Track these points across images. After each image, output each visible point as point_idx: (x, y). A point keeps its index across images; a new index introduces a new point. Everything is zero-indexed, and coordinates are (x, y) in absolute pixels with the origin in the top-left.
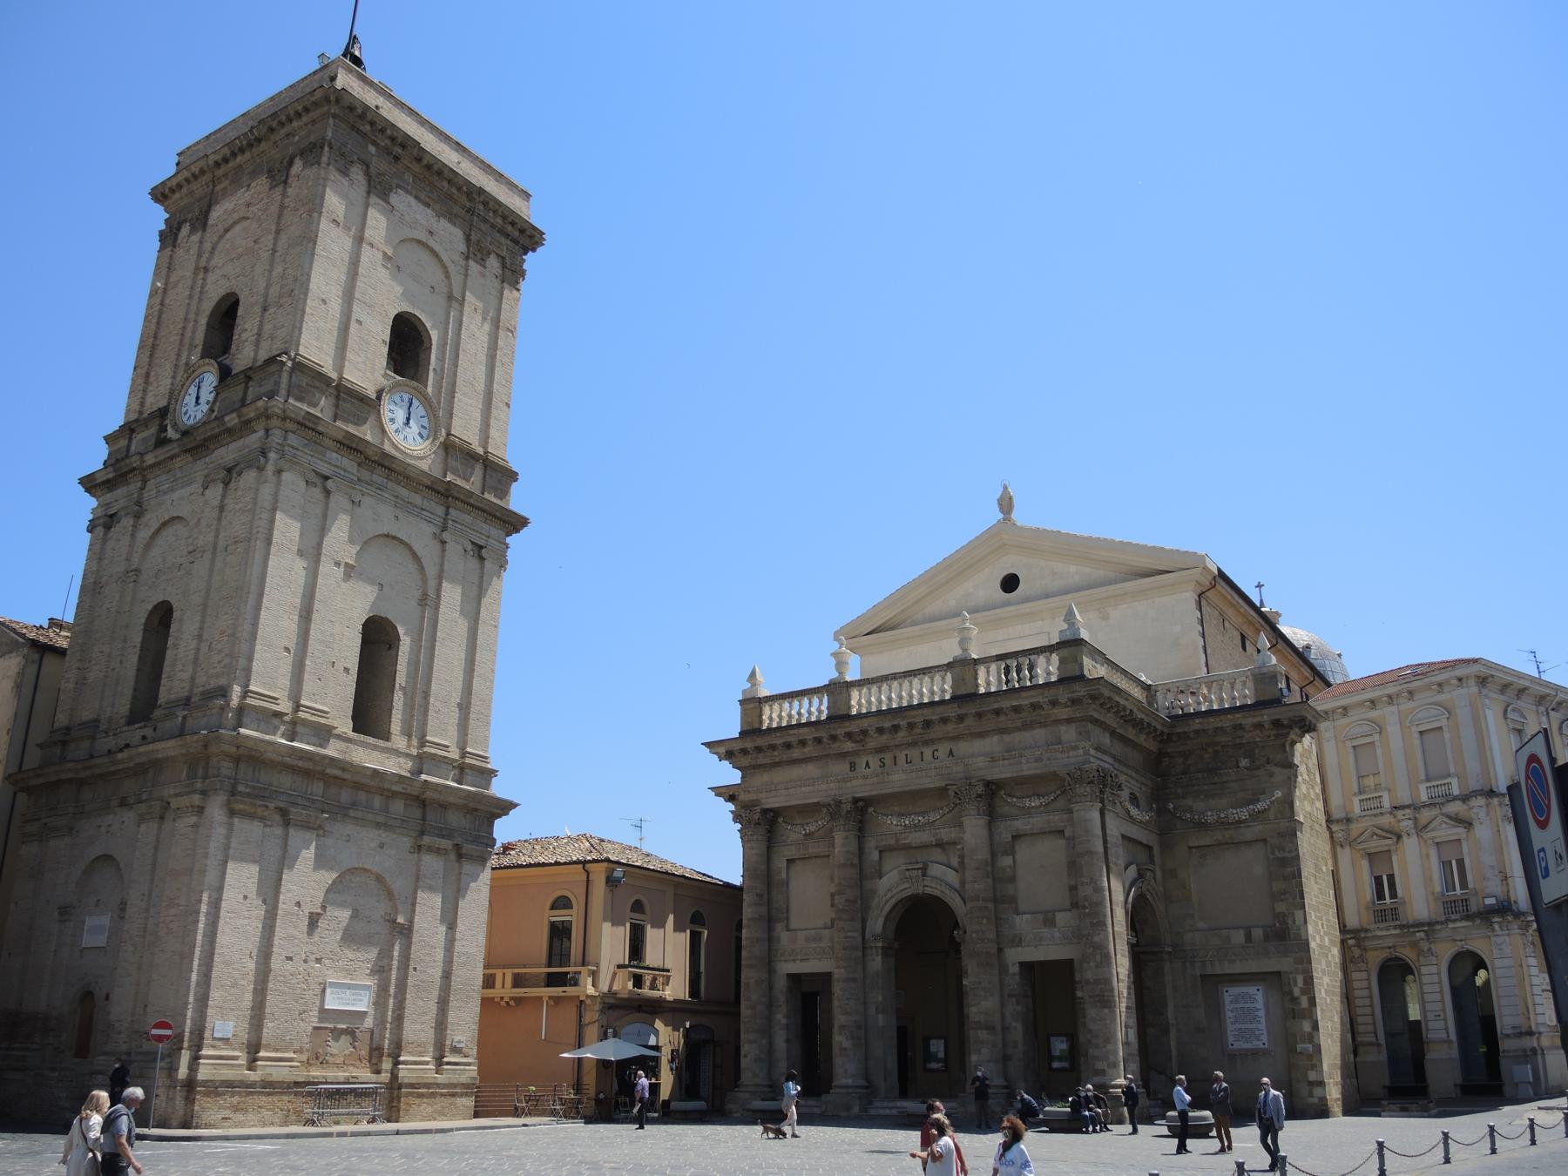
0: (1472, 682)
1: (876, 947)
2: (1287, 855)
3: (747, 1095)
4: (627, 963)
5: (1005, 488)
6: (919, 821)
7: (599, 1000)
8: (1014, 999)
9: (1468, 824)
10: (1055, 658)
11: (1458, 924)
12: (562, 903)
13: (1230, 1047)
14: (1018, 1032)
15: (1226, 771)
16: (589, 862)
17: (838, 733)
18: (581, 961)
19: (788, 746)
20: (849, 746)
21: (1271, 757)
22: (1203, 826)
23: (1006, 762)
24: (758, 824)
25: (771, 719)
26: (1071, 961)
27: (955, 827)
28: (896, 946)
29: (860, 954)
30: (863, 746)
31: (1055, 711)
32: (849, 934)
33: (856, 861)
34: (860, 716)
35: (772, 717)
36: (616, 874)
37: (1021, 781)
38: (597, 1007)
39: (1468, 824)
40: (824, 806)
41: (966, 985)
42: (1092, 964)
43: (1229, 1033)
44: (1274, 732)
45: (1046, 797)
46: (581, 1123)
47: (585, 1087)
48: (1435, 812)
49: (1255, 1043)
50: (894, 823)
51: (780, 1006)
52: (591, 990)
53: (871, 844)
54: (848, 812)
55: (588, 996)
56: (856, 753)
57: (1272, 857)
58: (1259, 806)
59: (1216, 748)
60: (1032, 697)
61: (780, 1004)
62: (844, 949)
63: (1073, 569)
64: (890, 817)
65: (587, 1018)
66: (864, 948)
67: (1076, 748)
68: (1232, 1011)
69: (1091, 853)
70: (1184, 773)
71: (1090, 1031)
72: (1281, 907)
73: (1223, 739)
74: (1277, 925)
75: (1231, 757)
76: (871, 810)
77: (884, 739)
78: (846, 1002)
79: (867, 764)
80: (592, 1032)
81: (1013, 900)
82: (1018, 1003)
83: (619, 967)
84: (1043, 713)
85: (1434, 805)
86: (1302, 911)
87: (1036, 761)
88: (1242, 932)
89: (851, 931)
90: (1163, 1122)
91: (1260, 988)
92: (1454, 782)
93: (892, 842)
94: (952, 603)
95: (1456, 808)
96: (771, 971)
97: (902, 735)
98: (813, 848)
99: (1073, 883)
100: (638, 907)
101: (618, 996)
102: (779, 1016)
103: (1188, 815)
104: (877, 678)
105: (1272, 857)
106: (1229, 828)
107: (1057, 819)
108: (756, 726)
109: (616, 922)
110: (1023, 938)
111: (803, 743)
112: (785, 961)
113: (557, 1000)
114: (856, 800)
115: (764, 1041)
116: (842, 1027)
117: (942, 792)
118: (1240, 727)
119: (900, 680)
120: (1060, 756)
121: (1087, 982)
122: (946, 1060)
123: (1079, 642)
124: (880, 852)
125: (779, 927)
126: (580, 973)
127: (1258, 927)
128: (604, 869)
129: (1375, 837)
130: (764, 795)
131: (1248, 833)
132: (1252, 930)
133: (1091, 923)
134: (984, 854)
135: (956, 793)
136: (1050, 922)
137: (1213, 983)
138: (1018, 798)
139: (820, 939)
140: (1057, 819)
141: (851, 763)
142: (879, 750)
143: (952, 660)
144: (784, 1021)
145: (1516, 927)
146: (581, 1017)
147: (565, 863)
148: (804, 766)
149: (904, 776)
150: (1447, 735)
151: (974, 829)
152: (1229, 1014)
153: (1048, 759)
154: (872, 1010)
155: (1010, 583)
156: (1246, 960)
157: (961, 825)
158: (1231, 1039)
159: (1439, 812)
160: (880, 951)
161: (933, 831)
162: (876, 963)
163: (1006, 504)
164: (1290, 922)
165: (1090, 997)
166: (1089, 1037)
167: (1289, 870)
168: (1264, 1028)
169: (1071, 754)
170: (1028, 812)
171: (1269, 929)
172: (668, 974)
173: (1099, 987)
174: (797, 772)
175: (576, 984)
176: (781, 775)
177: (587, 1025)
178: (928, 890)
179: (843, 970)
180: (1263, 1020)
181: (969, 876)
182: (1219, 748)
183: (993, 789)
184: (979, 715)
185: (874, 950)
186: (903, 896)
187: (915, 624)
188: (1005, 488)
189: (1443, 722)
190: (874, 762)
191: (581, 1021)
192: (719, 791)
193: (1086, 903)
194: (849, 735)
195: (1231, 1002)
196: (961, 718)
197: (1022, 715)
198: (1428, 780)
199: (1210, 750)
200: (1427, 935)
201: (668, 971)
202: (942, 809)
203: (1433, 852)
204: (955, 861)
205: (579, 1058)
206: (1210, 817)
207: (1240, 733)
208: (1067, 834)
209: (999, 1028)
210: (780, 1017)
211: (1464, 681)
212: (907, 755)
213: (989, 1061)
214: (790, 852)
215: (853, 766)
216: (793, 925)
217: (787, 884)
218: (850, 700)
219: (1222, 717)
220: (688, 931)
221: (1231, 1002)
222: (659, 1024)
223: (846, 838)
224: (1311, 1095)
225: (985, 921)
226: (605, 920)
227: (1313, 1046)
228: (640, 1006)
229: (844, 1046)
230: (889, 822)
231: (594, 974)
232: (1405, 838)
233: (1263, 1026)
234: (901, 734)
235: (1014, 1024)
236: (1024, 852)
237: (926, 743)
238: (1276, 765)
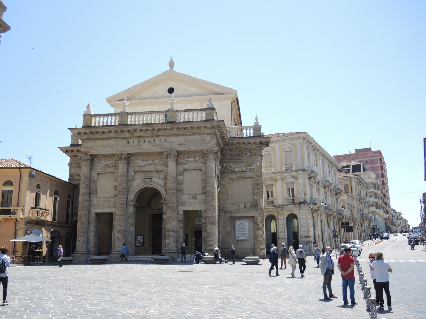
0: (302, 139)
1: (131, 205)
2: (259, 182)
3: (80, 255)
4: (34, 207)
5: (172, 59)
6: (150, 163)
7: (24, 220)
8: (180, 222)
9: (296, 178)
10: (204, 113)
11: (291, 206)
12: (9, 183)
13: (237, 238)
14: (181, 233)
15: (243, 156)
16: (22, 168)
17: (125, 129)
18: (17, 205)
19: (104, 133)
20: (127, 135)
21: (257, 153)
22: (234, 172)
23: (185, 145)
24: (88, 159)
25: (95, 123)
26: (200, 211)
27: (163, 165)
28: (137, 204)
29: (126, 206)
30: (133, 135)
31: (205, 130)
32: (123, 199)
33: (126, 175)
34: (131, 125)
35: (95, 122)
36: (33, 173)
37: (188, 152)
38: (24, 223)
39: (296, 178)
40: (116, 155)
41: (164, 218)
42: (211, 211)
43: (237, 234)
44: (259, 145)
45: (196, 158)
46: (22, 266)
47: (17, 252)
48: (287, 174)
49: (245, 237)
50: (141, 163)
51: (92, 224)
52: (22, 216)
53: (131, 170)
54: (125, 158)
55: (21, 219)
56: (129, 138)
57: (254, 182)
58: (252, 167)
59: (240, 149)
60: (198, 124)
61: (92, 223)
62: (121, 204)
63: (193, 89)
64: (139, 161)
65: (19, 226)
66: (127, 204)
67: (210, 143)
68: (238, 228)
69: (212, 176)
70: (230, 155)
71: (208, 232)
72: (256, 197)
73: (243, 146)
74: (254, 203)
75: (245, 152)
76: (132, 158)
77: (141, 134)
78: (120, 222)
79: (134, 142)
80: (21, 232)
81: (182, 190)
82: (182, 224)
83: (32, 208)
84: (200, 130)
85: (287, 172)
86: (262, 199)
87: (196, 146)
88: (244, 204)
89: (123, 199)
90: (244, 260)
91: (247, 221)
92: (294, 166)
93: (139, 169)
94: (150, 94)
95: (293, 173)
96: (90, 212)
97: (148, 133)
98: (108, 170)
99: (203, 186)
100: (38, 186)
101: (31, 219)
102: (92, 227)
103: (230, 168)
104: (139, 112)
105: (254, 182)
106: (242, 173)
108: (89, 125)
109: (31, 192)
110: (185, 203)
111: (110, 132)
112: (95, 208)
113: (6, 220)
114: (128, 154)
115: (86, 236)
116: (119, 231)
117: (161, 153)
118: (250, 143)
119: (148, 114)
120: (204, 145)
121: (208, 217)
122: (143, 243)
123: (213, 109)
124: (135, 172)
125: (93, 197)
126: (17, 210)
127: (248, 203)
128: (29, 171)
129: (269, 180)
130: (91, 149)
132: (247, 204)
133: (211, 198)
134: (174, 175)
135: (167, 154)
136: (195, 198)
137: (233, 219)
138: (187, 158)
139: (109, 201)
141: (127, 141)
142: (139, 137)
143: (168, 109)
144: (93, 229)
145: (307, 207)
146: (16, 226)
147: (11, 168)
148: (108, 140)
149: (147, 147)
150: (293, 153)
151: (172, 166)
152: (237, 229)
153: (200, 145)
154: (129, 226)
155: (171, 90)
156: (244, 212)
157: (167, 166)
158: (237, 236)
159: (288, 174)
160: (132, 206)
161: (155, 167)
162: (131, 209)
163: (172, 64)
164: (258, 202)
165: (210, 222)
166: (208, 234)
167: (259, 187)
168: (248, 233)
169: (208, 144)
170: (189, 162)
171: (252, 204)
172: (49, 211)
173: (213, 219)
174: (105, 142)
175: (15, 214)
176: (99, 143)
177: (19, 229)
178: (152, 186)
179: (120, 212)
180: (247, 231)
181: (169, 182)
182: (241, 149)
183: (179, 153)
184: (178, 129)
185: (130, 205)
186: (142, 188)
187: (136, 99)
188: (172, 59)
189: (292, 149)
190: (136, 141)
191: (16, 228)
192: (61, 149)
193: (210, 192)
194: (128, 131)
195: (238, 225)
196: (171, 129)
197: (193, 130)
198: (286, 165)
199: (239, 149)
200: (281, 209)
201: (48, 210)
202: (159, 159)
203: (285, 186)
204: (162, 177)
205: (15, 241)
206: (237, 170)
207: (249, 145)
208: (202, 170)
209: (176, 232)
210: (92, 228)
211: (300, 138)
213: (173, 242)
214: (99, 171)
215: (128, 142)
216: (98, 196)
217: (97, 182)
218: (128, 119)
219: (245, 139)
220: (53, 197)
221: (238, 225)
222: (43, 230)
223: (124, 167)
224: (261, 253)
225: (174, 197)
226: (28, 190)
227: (262, 239)
228: (37, 223)
229: (119, 237)
230: (139, 162)
231: (23, 210)
232: (278, 181)
233: (247, 232)
234: (148, 132)
235: (180, 230)
236: (187, 175)
237: (157, 136)
238: (258, 155)
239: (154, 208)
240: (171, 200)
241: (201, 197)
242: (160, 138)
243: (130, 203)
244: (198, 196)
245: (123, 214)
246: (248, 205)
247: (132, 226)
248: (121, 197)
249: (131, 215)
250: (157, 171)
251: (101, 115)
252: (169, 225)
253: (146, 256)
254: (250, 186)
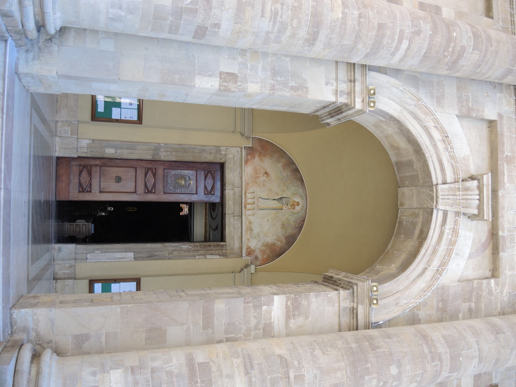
1: (351, 93)
32: (405, 45)
41: (270, 303)
62: (381, 27)
89: (408, 48)
239: (248, 170)
240: (400, 373)
243: (358, 87)
245: (322, 37)
247: (224, 90)
248: (418, 33)
249: (293, 88)
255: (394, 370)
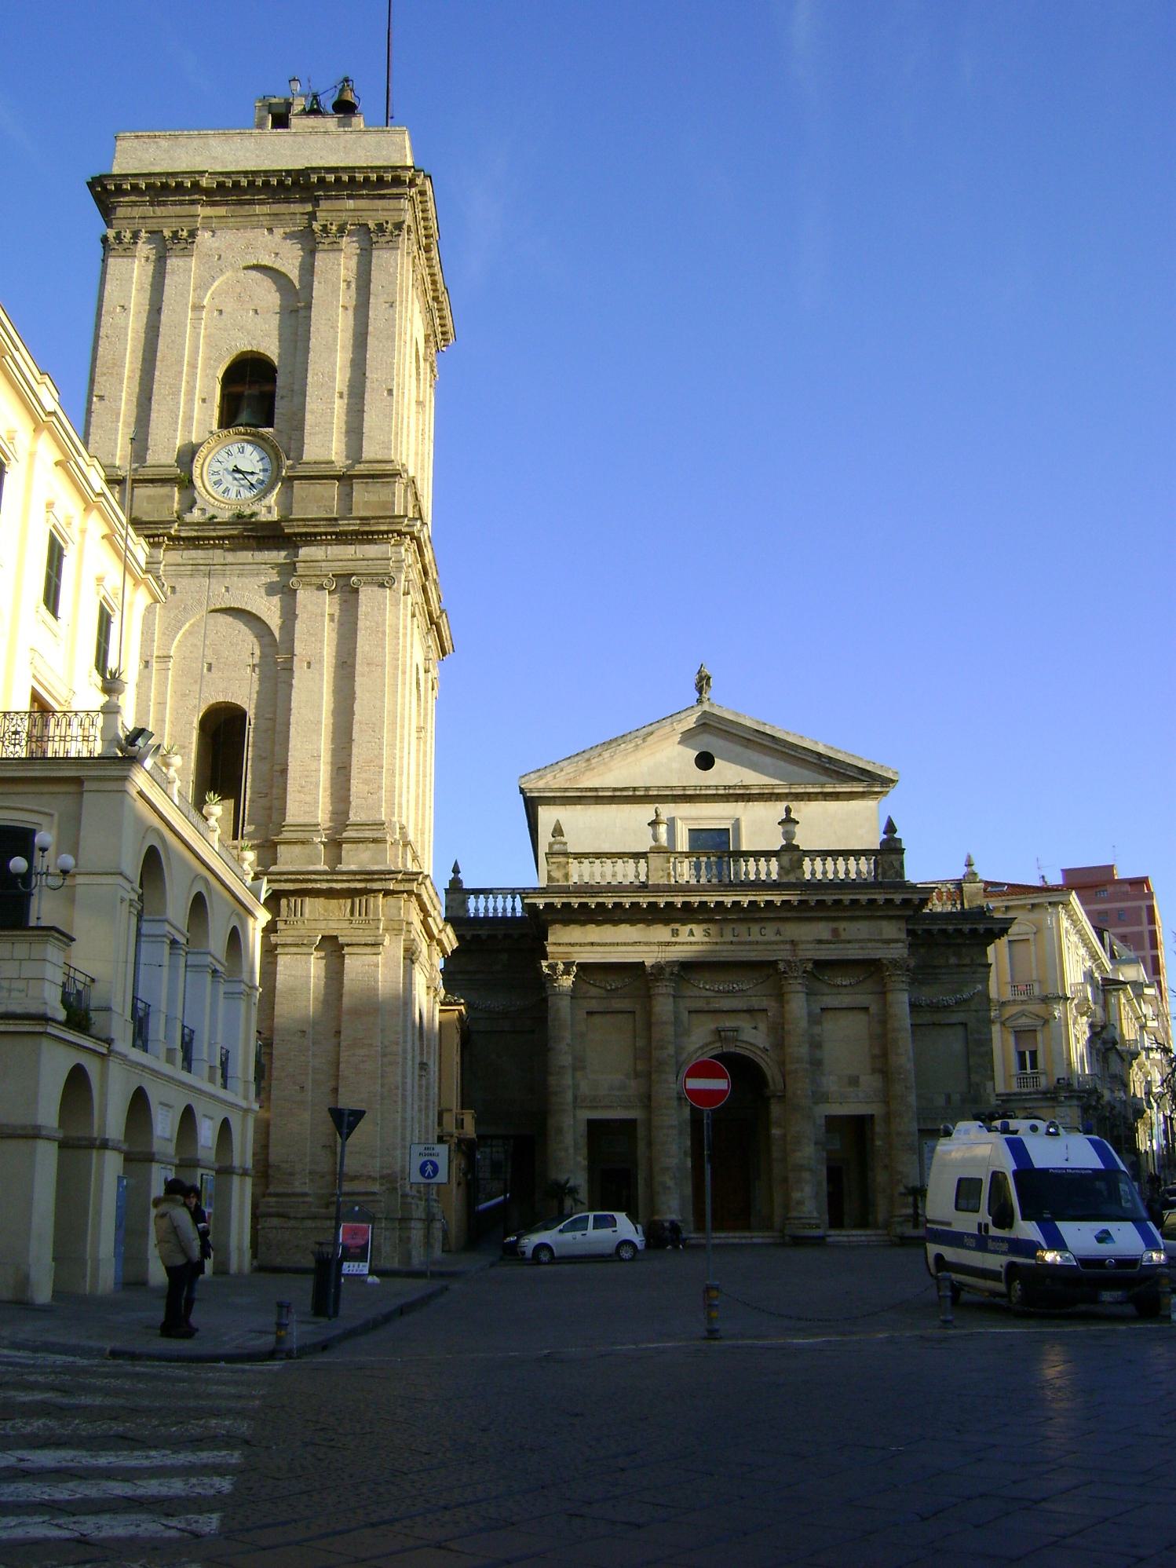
72: (975, 1078)
107: (862, 999)
121: (899, 1134)
131: (955, 1018)
140: (862, 999)
141: (673, 930)
164: (982, 1091)
166: (899, 1177)
189: (1031, 937)
203: (1011, 1039)
208: (872, 1010)
212: (733, 929)
241: (870, 1082)
242: (763, 925)
244: (862, 1079)
246: (956, 1098)
250: (749, 1011)
251: (598, 855)
252: (799, 1154)
253: (737, 1234)
254: (958, 1046)
255: (799, 1092)
